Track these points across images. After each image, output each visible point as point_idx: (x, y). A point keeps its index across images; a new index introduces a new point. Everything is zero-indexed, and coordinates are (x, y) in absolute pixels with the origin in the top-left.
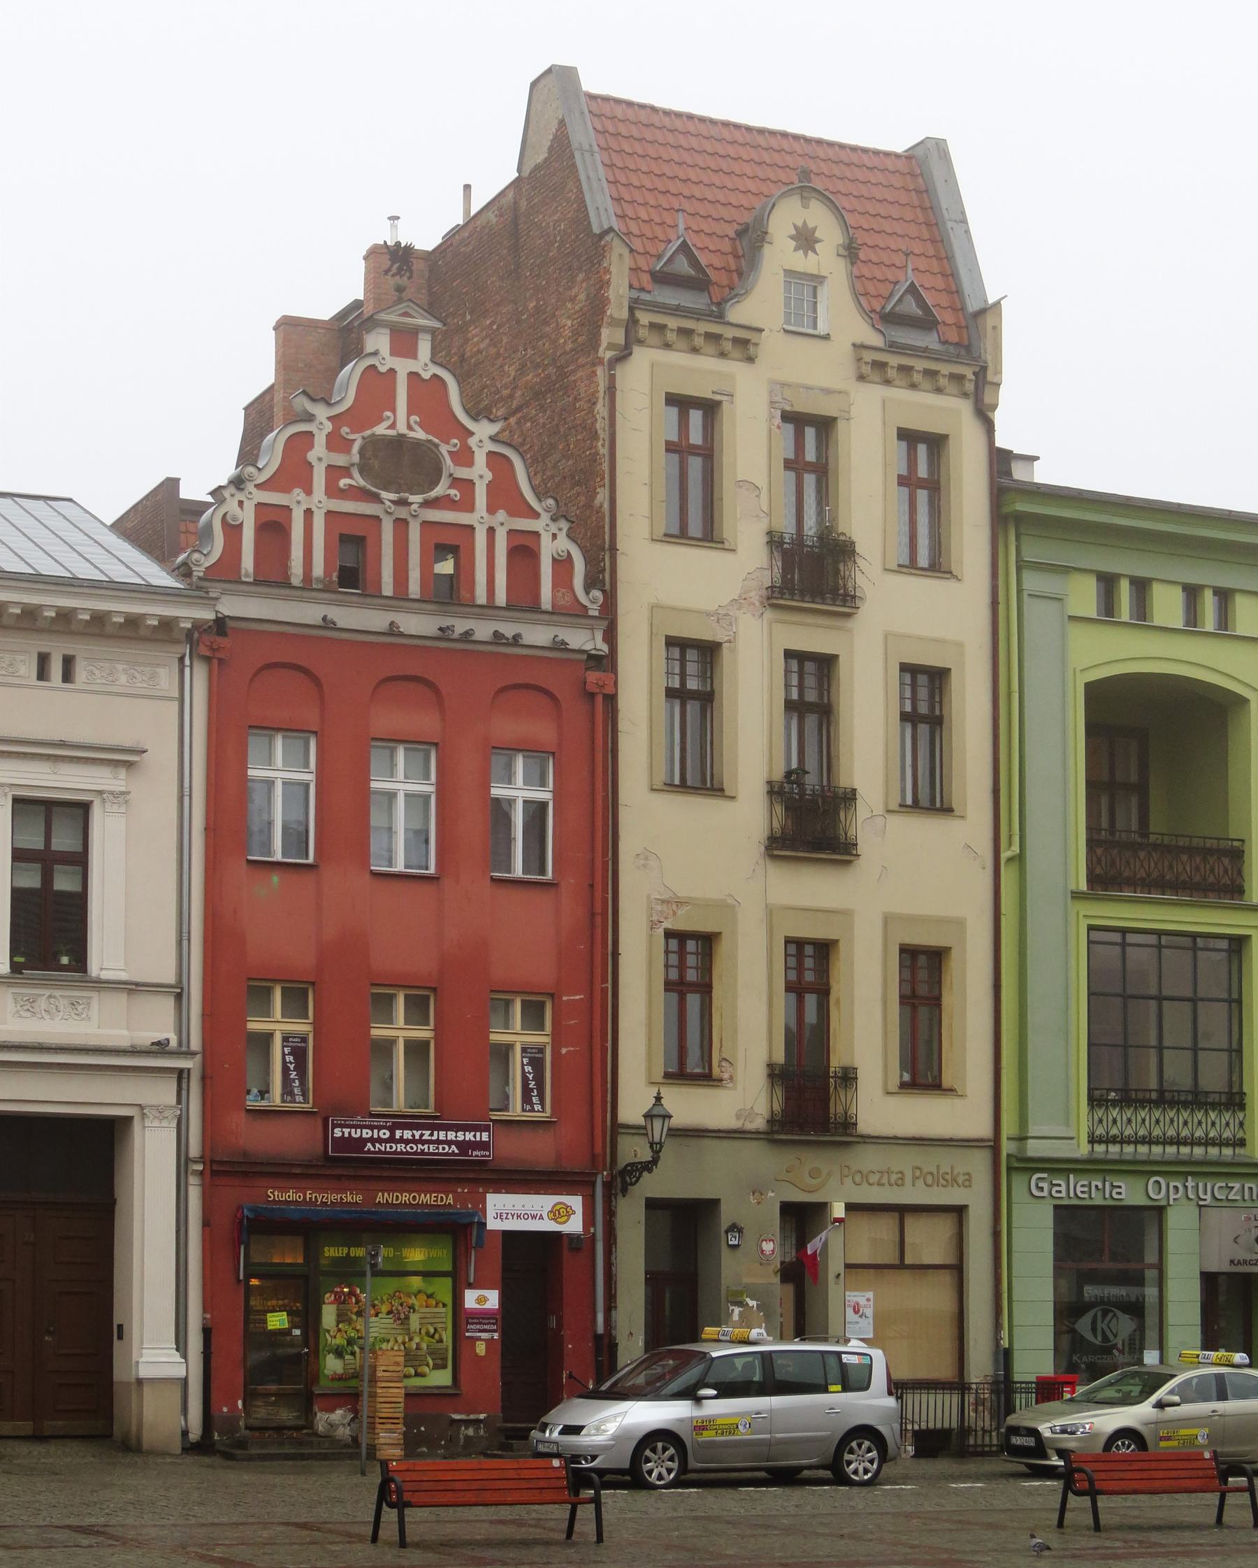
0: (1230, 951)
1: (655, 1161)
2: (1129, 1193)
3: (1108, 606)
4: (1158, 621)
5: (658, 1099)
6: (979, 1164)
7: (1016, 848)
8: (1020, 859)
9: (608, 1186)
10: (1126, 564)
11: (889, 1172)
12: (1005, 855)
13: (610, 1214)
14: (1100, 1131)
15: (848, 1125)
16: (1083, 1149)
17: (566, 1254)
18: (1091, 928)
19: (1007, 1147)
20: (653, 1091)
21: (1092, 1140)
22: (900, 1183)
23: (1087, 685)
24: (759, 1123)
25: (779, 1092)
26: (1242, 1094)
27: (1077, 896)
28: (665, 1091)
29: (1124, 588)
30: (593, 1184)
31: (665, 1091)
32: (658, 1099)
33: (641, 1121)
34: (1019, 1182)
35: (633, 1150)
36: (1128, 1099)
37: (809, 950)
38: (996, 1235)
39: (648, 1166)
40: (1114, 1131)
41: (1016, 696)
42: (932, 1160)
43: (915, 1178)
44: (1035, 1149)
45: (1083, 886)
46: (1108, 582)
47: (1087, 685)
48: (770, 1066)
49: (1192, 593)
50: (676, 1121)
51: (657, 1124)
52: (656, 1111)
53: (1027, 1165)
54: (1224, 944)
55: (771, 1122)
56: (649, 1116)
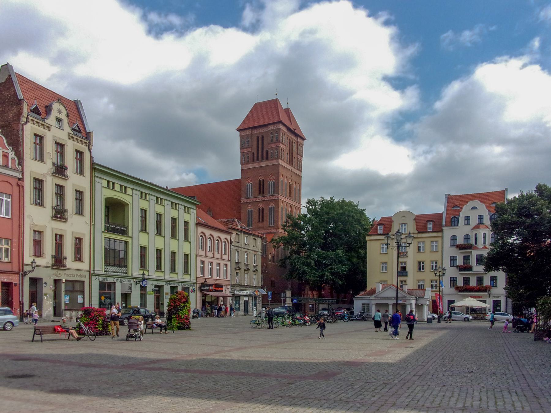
0: (125, 243)
1: (33, 271)
2: (111, 280)
3: (108, 186)
4: (116, 190)
5: (34, 259)
6: (87, 274)
7: (94, 223)
8: (94, 225)
9: (22, 274)
10: (112, 180)
11: (72, 275)
12: (92, 224)
13: (22, 279)
14: (105, 270)
15: (65, 266)
16: (103, 273)
17: (14, 287)
18: (105, 237)
19: (92, 272)
20: (33, 258)
21: (105, 271)
22: (74, 276)
23: (105, 198)
24: (50, 265)
25: (54, 260)
26: (126, 266)
27: (103, 232)
28: (35, 258)
29: (111, 183)
30: (19, 274)
31: (35, 258)
32: (34, 259)
33: (30, 264)
34: (93, 277)
35: (26, 268)
36: (109, 265)
37: (58, 236)
38: (90, 286)
39: (31, 271)
40: (108, 270)
41: (94, 198)
42: (79, 273)
43: (77, 276)
44: (96, 272)
45: (104, 231)
46: (108, 182)
47: (105, 198)
48: (52, 255)
49: (121, 186)
50: (37, 264)
51: (34, 264)
52: (33, 262)
53: (94, 275)
54: (124, 242)
55: (52, 265)
56: (32, 263)
